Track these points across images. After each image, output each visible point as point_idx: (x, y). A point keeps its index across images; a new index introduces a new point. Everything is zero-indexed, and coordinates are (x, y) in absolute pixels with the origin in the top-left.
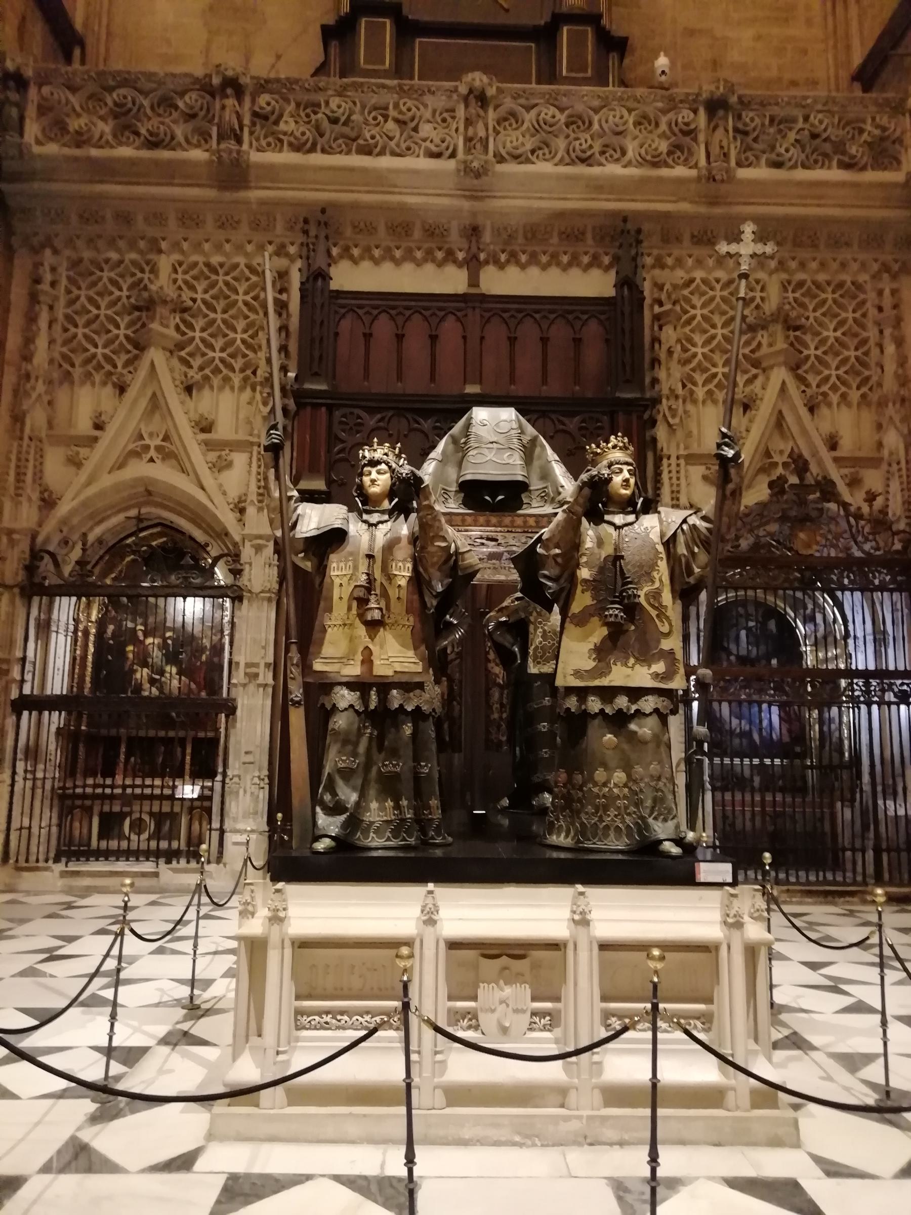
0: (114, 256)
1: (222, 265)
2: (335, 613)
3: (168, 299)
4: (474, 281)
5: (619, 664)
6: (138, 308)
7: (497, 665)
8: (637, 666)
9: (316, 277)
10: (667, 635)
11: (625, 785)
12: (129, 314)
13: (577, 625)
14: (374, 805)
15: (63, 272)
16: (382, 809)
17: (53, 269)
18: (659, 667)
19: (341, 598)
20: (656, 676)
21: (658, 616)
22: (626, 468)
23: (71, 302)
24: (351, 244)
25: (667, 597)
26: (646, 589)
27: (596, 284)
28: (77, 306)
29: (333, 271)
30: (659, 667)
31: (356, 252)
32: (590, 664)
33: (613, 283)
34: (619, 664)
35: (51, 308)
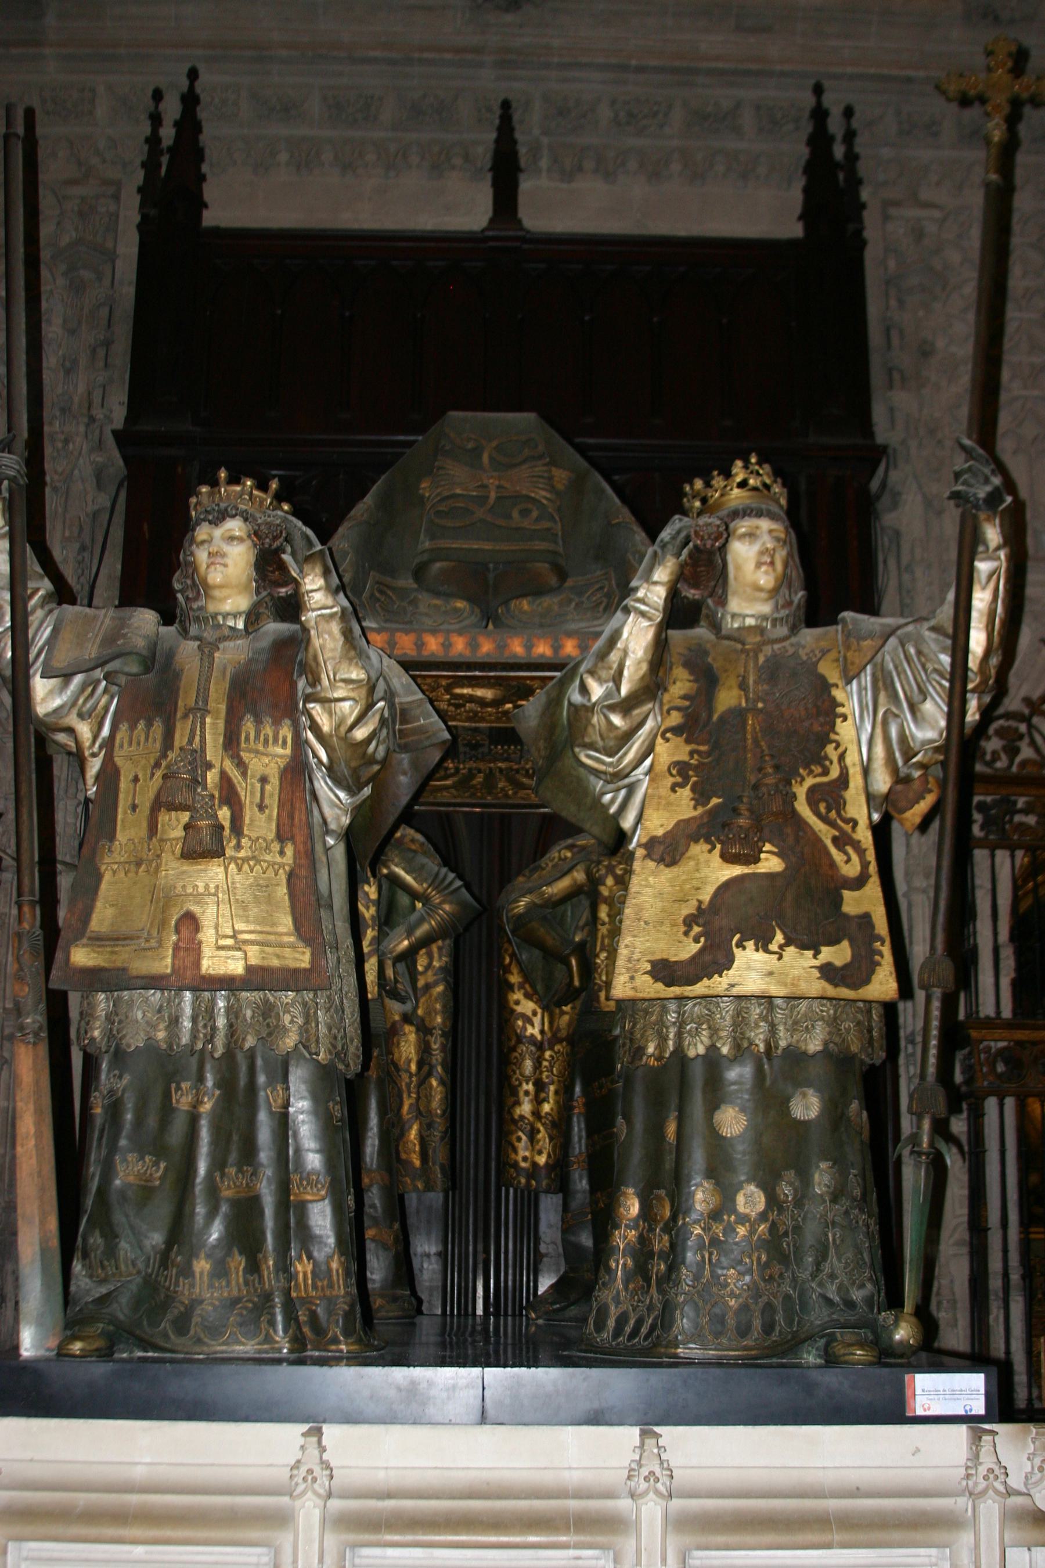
2: (121, 837)
5: (750, 944)
7: (528, 996)
8: (791, 950)
10: (859, 882)
11: (763, 1216)
13: (661, 860)
14: (202, 1266)
16: (220, 1271)
19: (134, 807)
20: (827, 972)
21: (835, 840)
22: (765, 524)
26: (810, 782)
27: (766, 210)
29: (210, 192)
30: (838, 954)
32: (689, 949)
33: (798, 210)
34: (750, 944)
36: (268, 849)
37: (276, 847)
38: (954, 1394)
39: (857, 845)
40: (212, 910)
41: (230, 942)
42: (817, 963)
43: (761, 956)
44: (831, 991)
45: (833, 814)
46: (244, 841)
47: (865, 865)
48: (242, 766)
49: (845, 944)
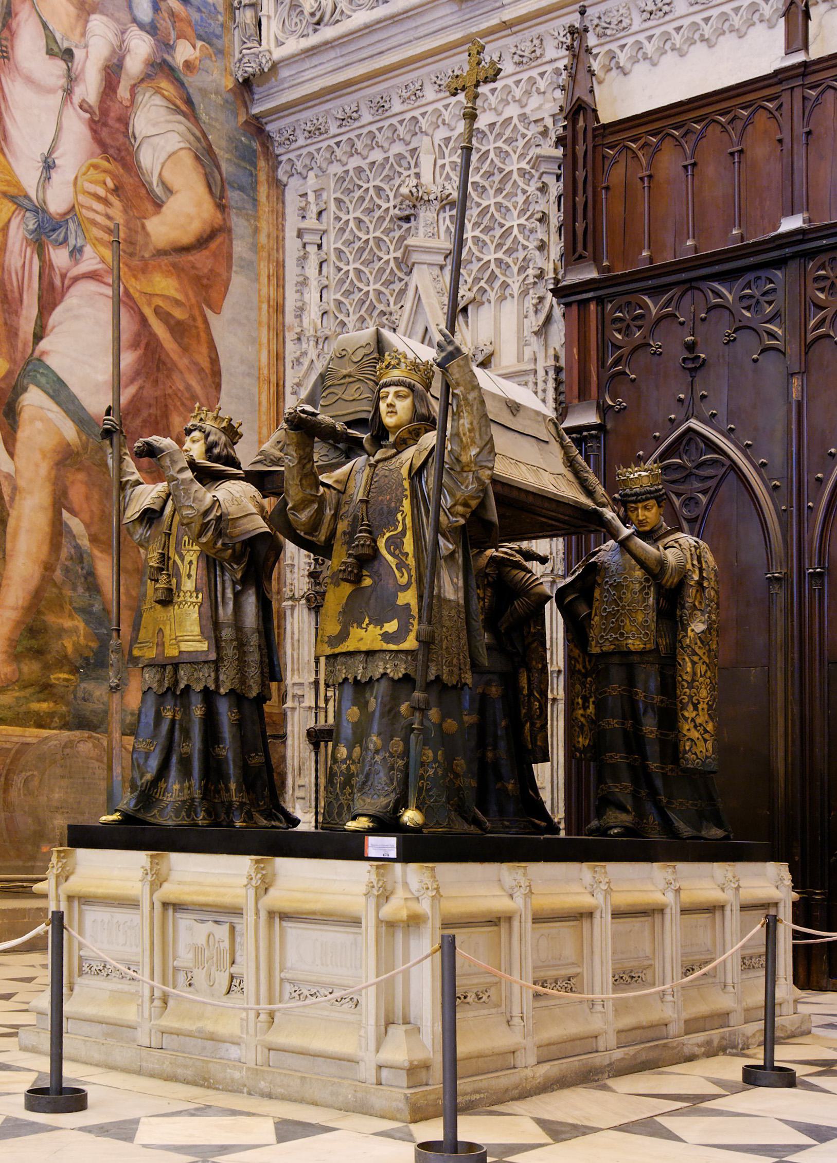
0: (377, 156)
1: (492, 125)
3: (432, 197)
4: (797, 37)
6: (407, 219)
9: (578, 111)
10: (405, 588)
12: (400, 227)
15: (330, 196)
17: (318, 193)
18: (392, 627)
20: (386, 637)
23: (342, 230)
24: (641, 37)
25: (408, 544)
28: (347, 235)
30: (392, 627)
31: (649, 48)
35: (320, 247)
36: (191, 597)
37: (194, 595)
38: (383, 847)
39: (407, 566)
40: (168, 627)
41: (174, 641)
42: (381, 632)
43: (359, 630)
44: (385, 646)
45: (397, 552)
46: (182, 594)
47: (410, 577)
48: (182, 558)
49: (396, 621)
